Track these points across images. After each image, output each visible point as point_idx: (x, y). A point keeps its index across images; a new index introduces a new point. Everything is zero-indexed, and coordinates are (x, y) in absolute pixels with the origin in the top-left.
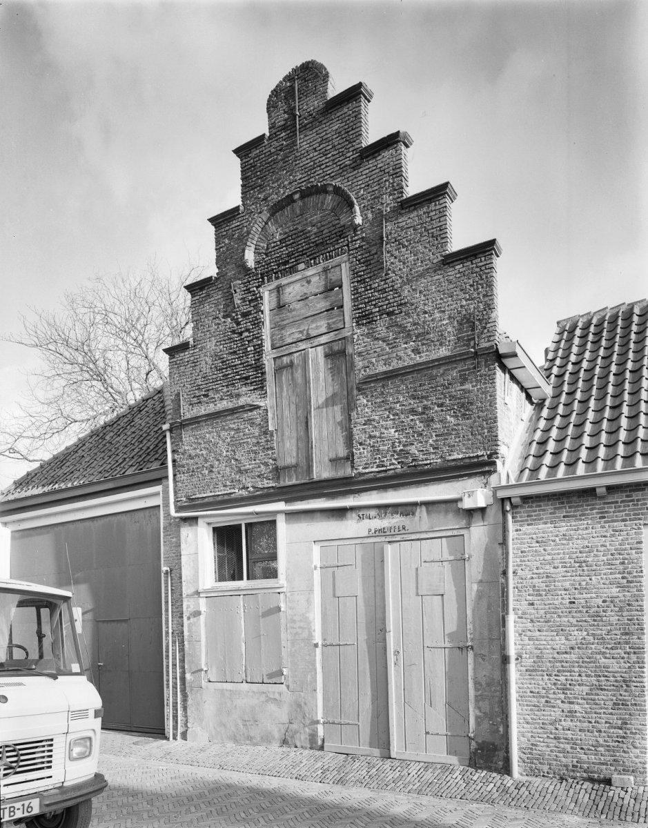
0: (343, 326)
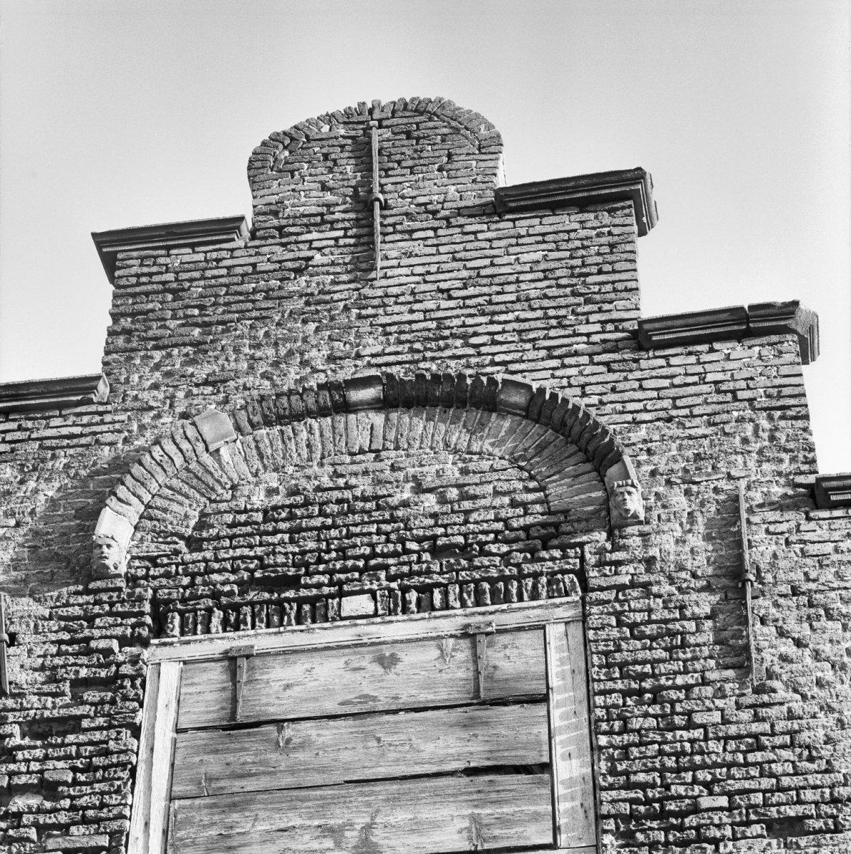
0: (549, 840)
